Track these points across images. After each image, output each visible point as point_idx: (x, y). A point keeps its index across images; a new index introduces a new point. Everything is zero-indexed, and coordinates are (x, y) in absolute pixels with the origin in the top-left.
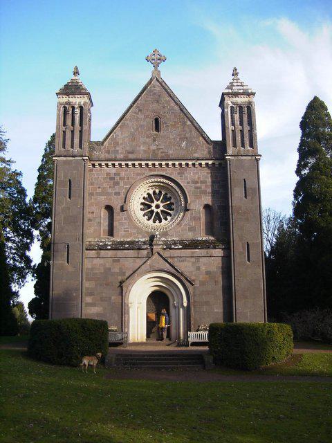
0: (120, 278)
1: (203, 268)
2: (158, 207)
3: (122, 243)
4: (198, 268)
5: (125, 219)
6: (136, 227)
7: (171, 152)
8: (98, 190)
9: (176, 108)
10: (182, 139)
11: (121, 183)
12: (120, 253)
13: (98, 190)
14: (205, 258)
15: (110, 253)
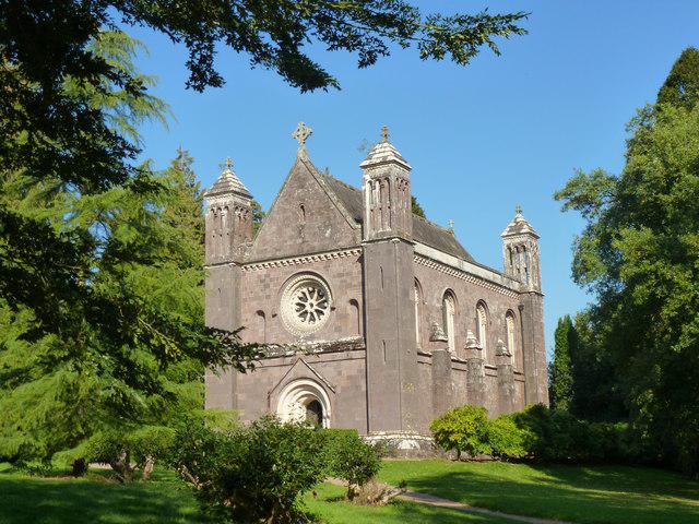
0: (268, 388)
2: (312, 305)
4: (340, 373)
7: (316, 244)
8: (251, 295)
10: (326, 227)
13: (251, 295)
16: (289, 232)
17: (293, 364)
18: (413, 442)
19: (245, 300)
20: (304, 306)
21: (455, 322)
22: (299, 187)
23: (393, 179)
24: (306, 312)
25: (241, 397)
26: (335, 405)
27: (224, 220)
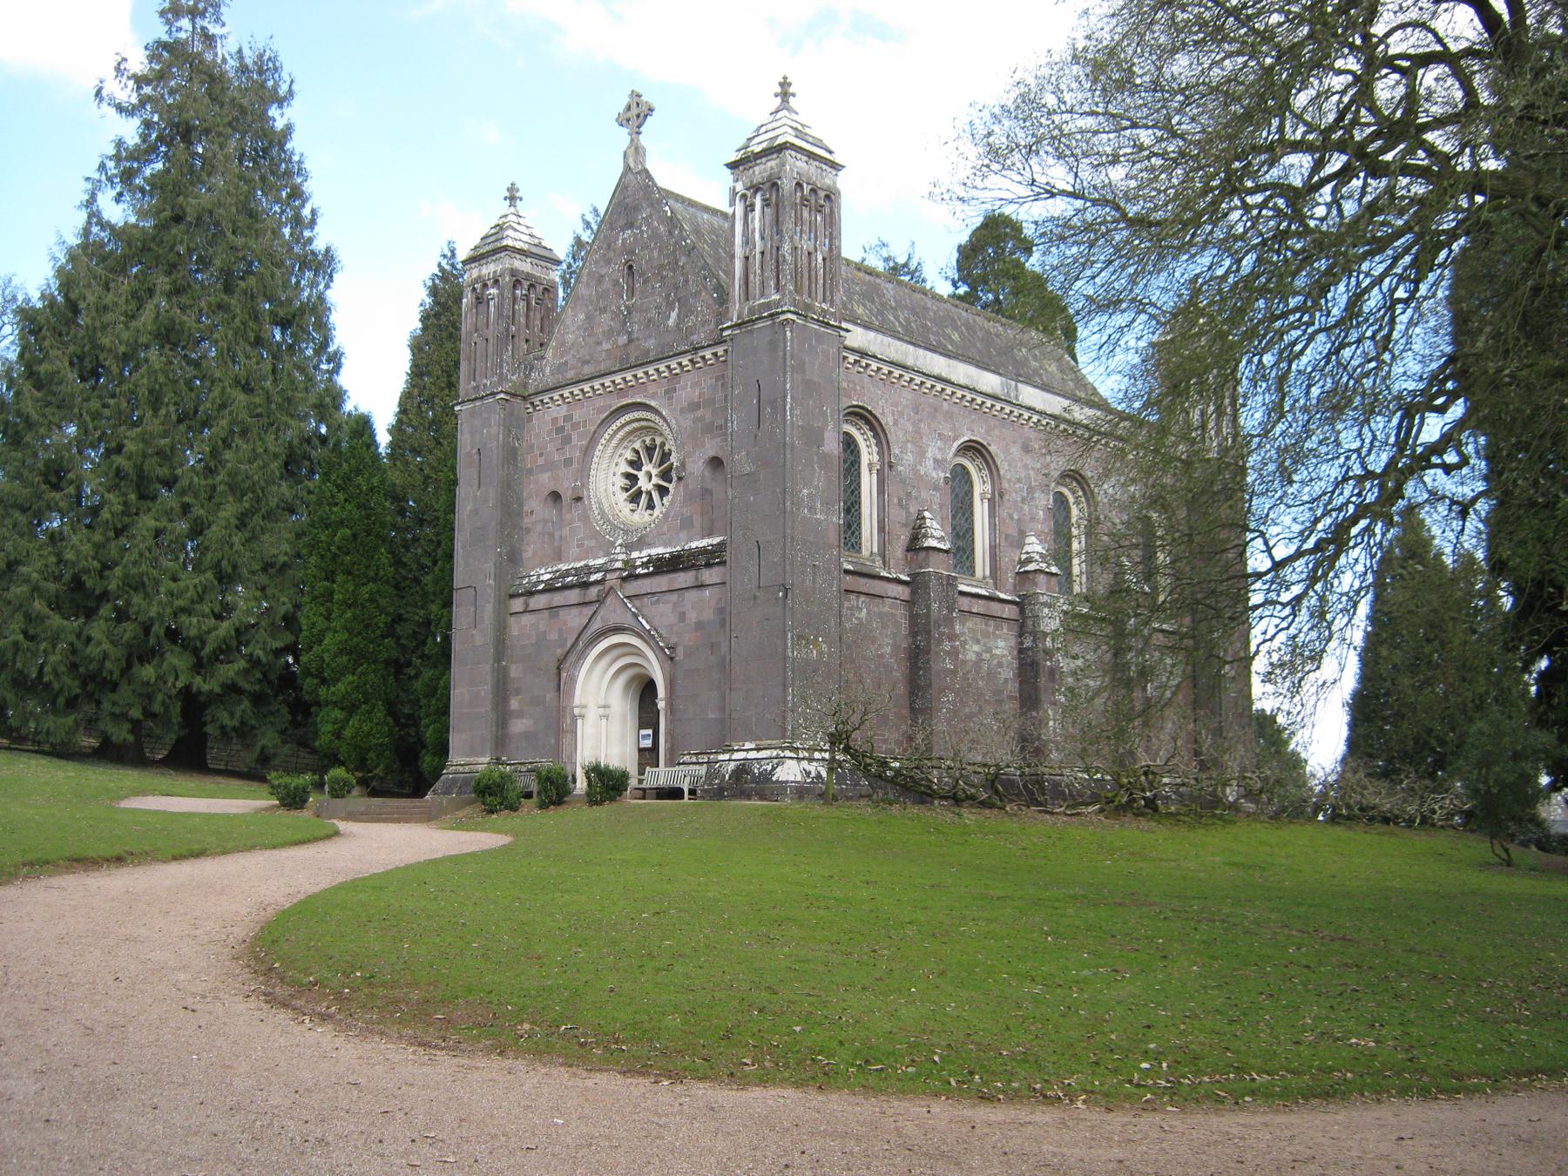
1: (692, 616)
3: (567, 573)
4: (682, 617)
6: (596, 535)
7: (651, 343)
8: (541, 461)
11: (574, 437)
12: (558, 599)
15: (539, 601)
16: (605, 321)
17: (600, 601)
18: (812, 768)
19: (530, 472)
21: (992, 514)
23: (787, 185)
24: (639, 492)
25: (515, 671)
26: (671, 684)
27: (492, 309)
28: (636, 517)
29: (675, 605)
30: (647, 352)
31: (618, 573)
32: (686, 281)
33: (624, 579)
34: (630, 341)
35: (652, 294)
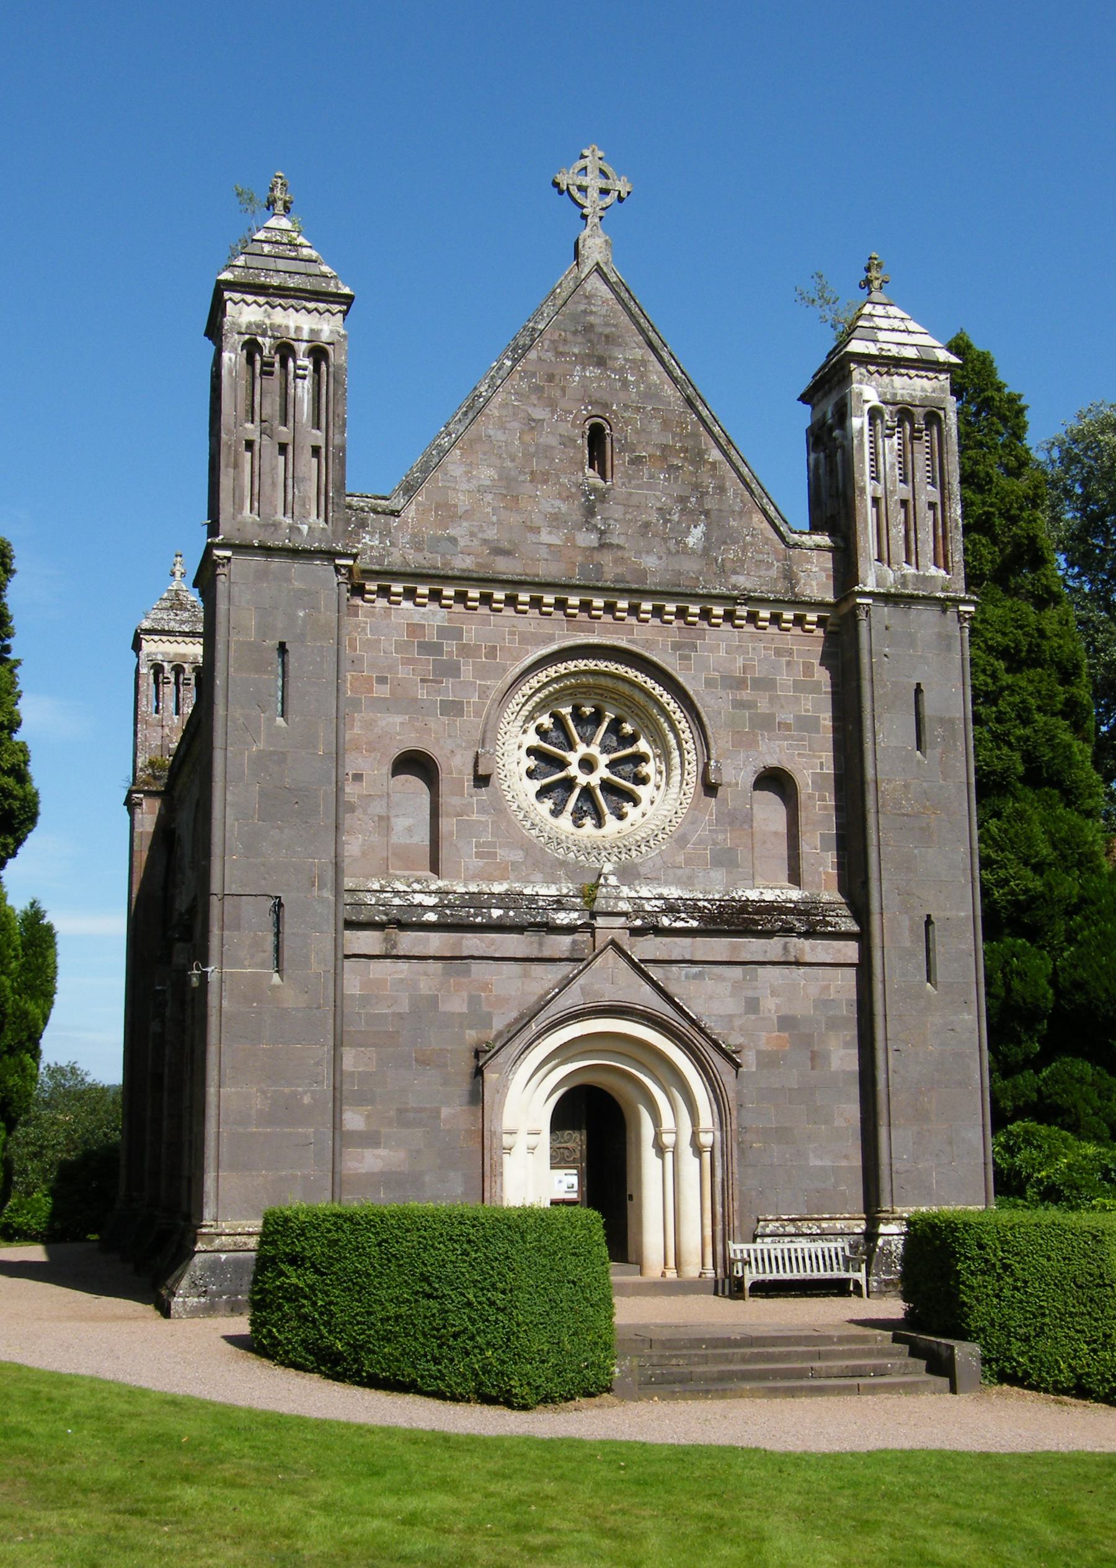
0: (472, 1036)
1: (770, 1005)
3: (475, 900)
4: (753, 1005)
5: (482, 810)
6: (527, 846)
7: (650, 562)
9: (669, 390)
10: (691, 516)
11: (467, 671)
12: (472, 943)
13: (382, 691)
14: (777, 971)
15: (435, 942)
20: (563, 764)
22: (584, 360)
28: (565, 821)
29: (737, 987)
30: (643, 574)
31: (621, 921)
32: (721, 489)
33: (635, 932)
34: (602, 546)
35: (650, 486)
